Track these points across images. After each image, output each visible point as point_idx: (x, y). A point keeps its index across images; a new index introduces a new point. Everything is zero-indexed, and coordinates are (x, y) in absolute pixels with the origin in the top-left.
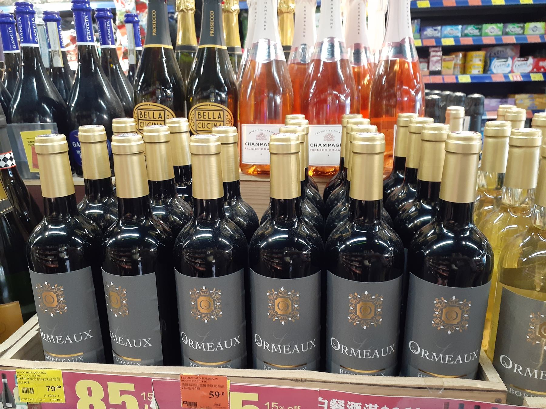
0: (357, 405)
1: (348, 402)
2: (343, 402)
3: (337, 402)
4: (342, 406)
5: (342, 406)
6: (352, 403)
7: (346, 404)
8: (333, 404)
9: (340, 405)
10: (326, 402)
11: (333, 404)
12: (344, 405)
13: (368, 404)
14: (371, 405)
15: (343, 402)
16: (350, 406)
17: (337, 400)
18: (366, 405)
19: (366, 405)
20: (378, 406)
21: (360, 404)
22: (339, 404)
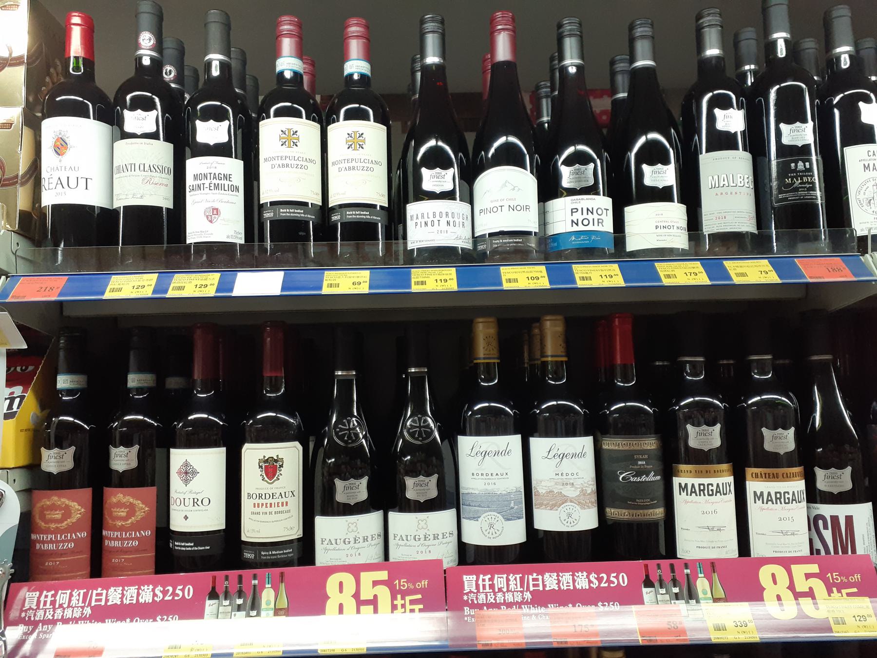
0: (134, 589)
1: (126, 588)
2: (121, 588)
3: (115, 590)
4: (119, 594)
5: (119, 594)
6: (129, 588)
7: (123, 590)
8: (111, 594)
9: (118, 593)
10: (104, 592)
11: (111, 594)
12: (121, 592)
13: (144, 587)
14: (146, 586)
15: (121, 588)
16: (127, 591)
17: (115, 588)
18: (142, 588)
19: (142, 588)
20: (153, 587)
21: (137, 587)
22: (117, 592)
